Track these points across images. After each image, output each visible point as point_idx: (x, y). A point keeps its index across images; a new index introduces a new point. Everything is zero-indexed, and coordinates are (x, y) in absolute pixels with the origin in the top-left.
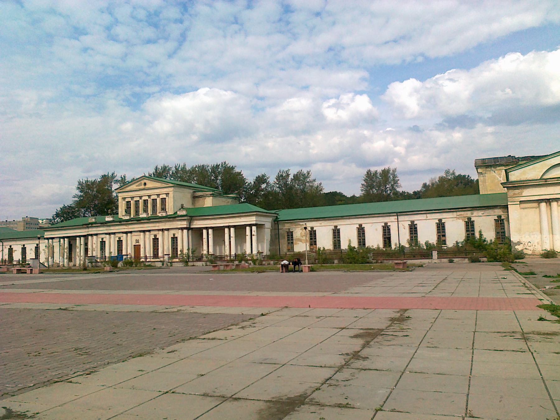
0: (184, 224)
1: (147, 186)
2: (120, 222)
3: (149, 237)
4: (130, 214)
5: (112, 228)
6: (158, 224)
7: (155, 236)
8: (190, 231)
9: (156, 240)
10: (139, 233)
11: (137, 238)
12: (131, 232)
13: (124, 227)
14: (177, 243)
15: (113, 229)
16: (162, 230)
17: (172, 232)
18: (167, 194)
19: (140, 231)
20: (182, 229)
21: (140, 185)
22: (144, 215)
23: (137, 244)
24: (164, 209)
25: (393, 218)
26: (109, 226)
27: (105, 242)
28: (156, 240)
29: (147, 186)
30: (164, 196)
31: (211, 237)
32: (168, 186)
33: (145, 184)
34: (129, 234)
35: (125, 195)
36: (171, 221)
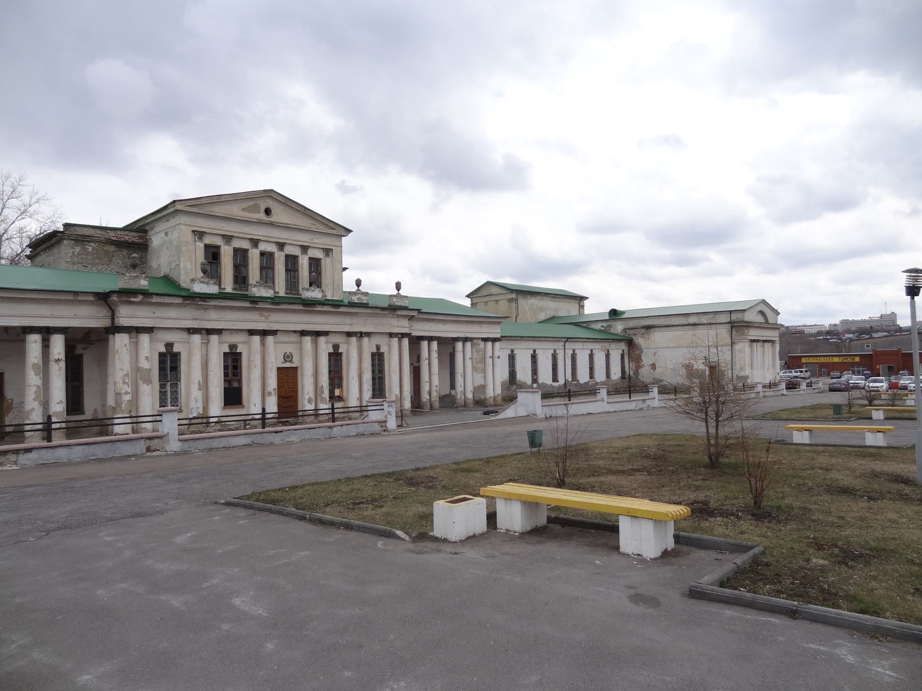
0: (401, 326)
1: (273, 218)
2: (252, 302)
3: (325, 346)
4: (218, 279)
5: (213, 314)
6: (348, 320)
7: (336, 347)
8: (469, 344)
9: (336, 357)
10: (294, 338)
11: (289, 349)
12: (274, 333)
13: (255, 316)
14: (373, 365)
15: (212, 319)
16: (361, 335)
17: (376, 340)
18: (328, 252)
19: (303, 333)
20: (403, 335)
21: (254, 209)
22: (315, 294)
23: (288, 365)
24: (315, 282)
25: (561, 344)
26: (206, 309)
27: (176, 357)
28: (336, 357)
29: (273, 218)
30: (319, 254)
31: (435, 355)
32: (334, 232)
33: (268, 212)
34: (270, 339)
35: (203, 224)
36: (377, 315)
